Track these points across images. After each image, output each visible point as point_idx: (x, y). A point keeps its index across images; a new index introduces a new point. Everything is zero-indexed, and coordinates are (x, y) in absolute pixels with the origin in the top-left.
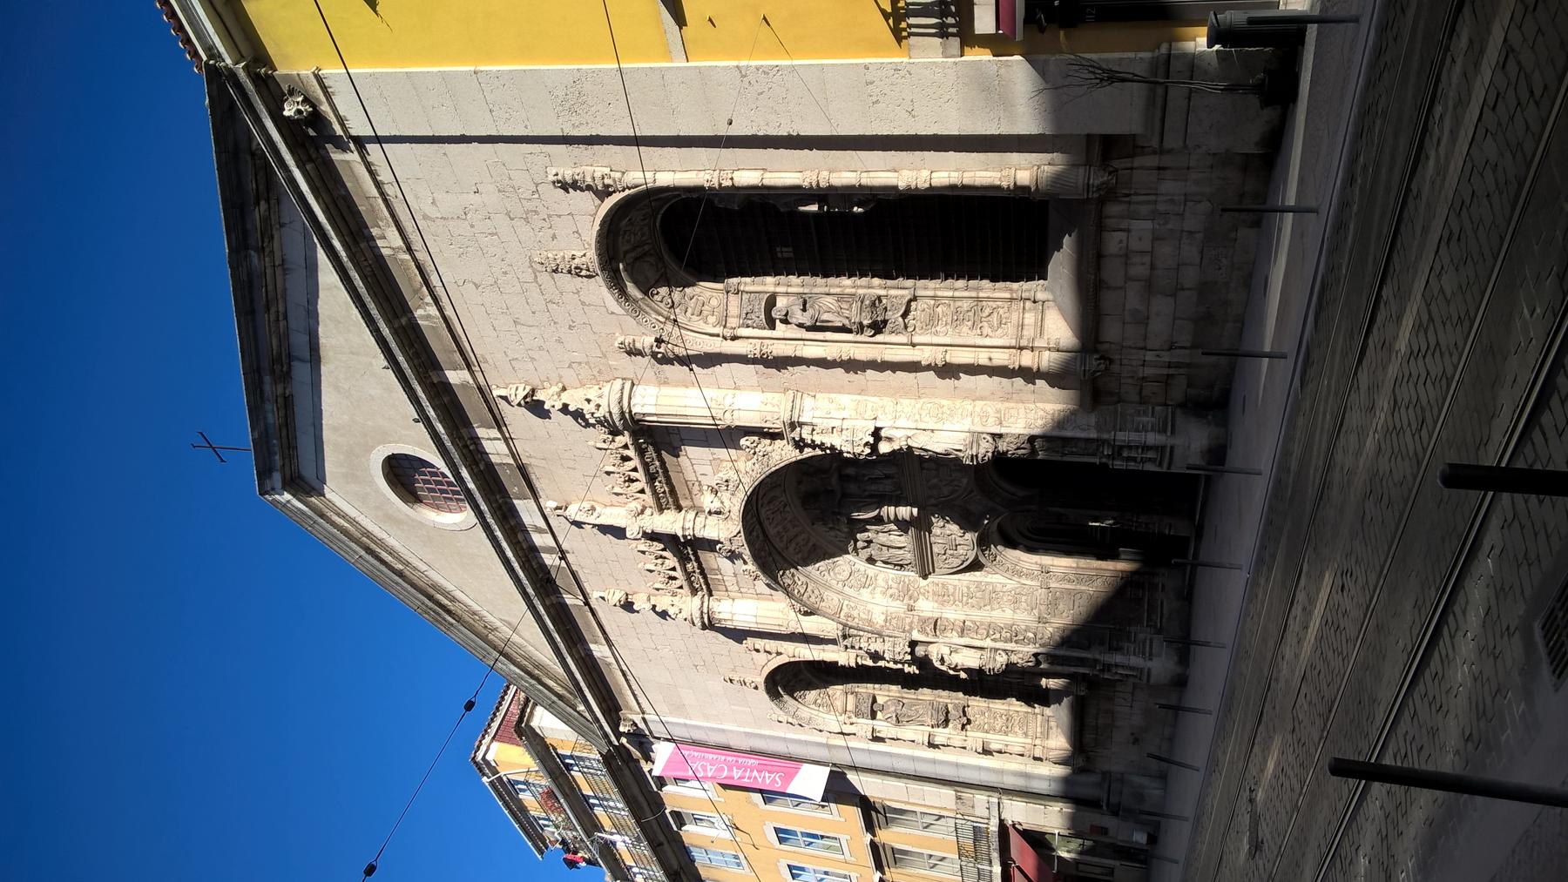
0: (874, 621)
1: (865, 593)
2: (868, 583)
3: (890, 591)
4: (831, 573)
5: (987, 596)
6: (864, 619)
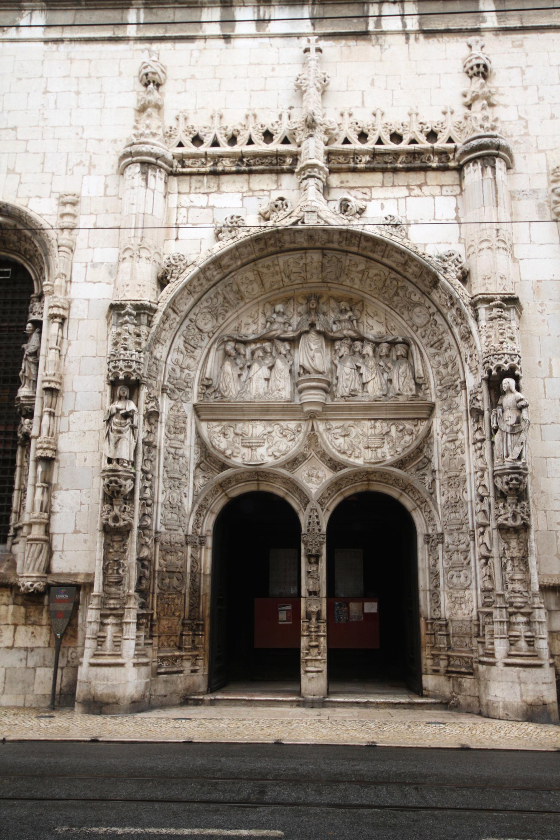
0: (157, 346)
1: (179, 342)
2: (189, 347)
3: (178, 370)
4: (205, 310)
5: (176, 476)
6: (161, 335)
